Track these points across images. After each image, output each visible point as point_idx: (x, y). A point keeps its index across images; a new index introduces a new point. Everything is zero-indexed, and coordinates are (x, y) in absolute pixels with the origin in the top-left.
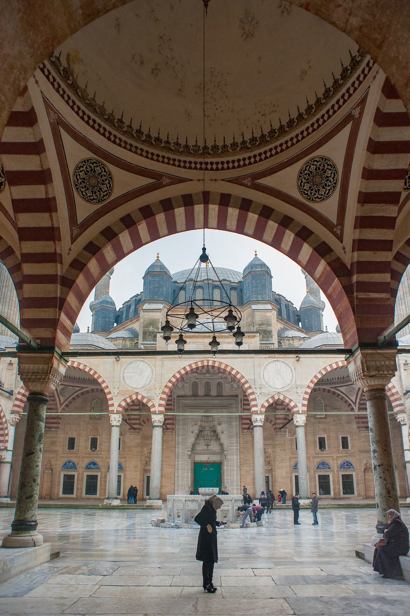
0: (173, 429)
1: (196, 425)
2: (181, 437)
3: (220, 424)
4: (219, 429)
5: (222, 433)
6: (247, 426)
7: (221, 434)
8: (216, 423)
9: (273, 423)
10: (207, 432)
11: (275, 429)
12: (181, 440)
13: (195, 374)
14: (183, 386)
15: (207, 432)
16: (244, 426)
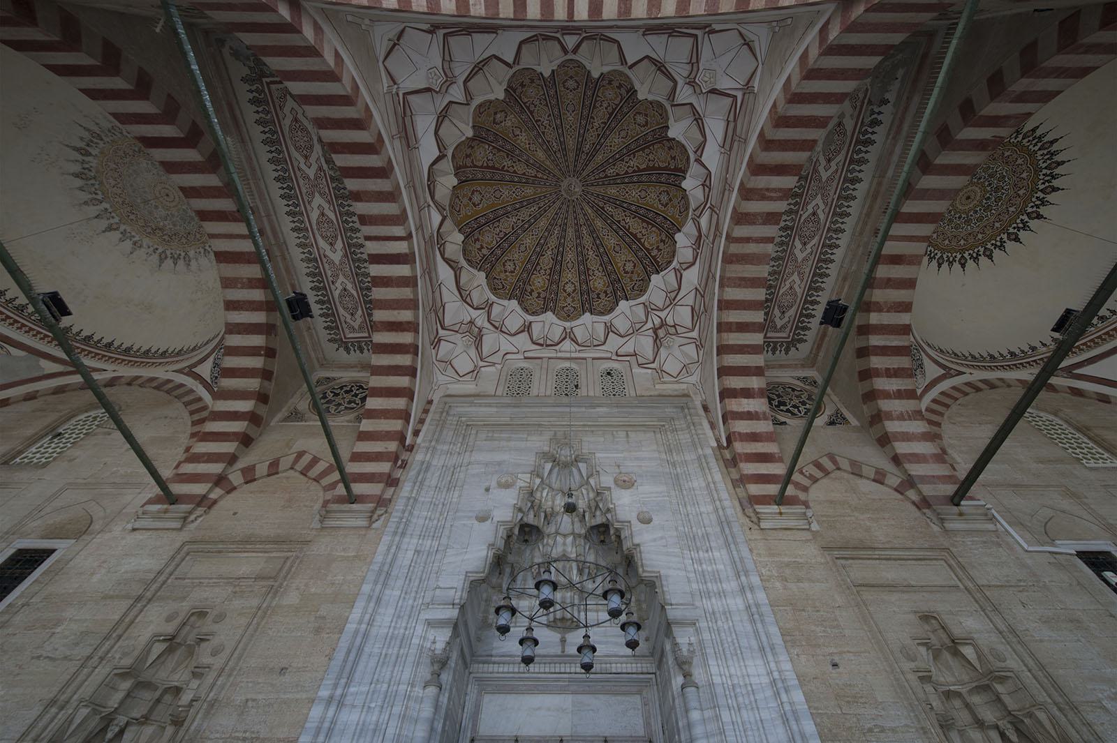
0: (382, 503)
1: (507, 486)
2: (410, 543)
3: (626, 483)
4: (625, 504)
5: (646, 521)
6: (773, 489)
7: (637, 526)
8: (607, 480)
9: (894, 480)
10: (564, 541)
11: (924, 503)
12: (406, 557)
13: (522, 341)
14: (475, 372)
15: (564, 541)
16: (755, 489)
